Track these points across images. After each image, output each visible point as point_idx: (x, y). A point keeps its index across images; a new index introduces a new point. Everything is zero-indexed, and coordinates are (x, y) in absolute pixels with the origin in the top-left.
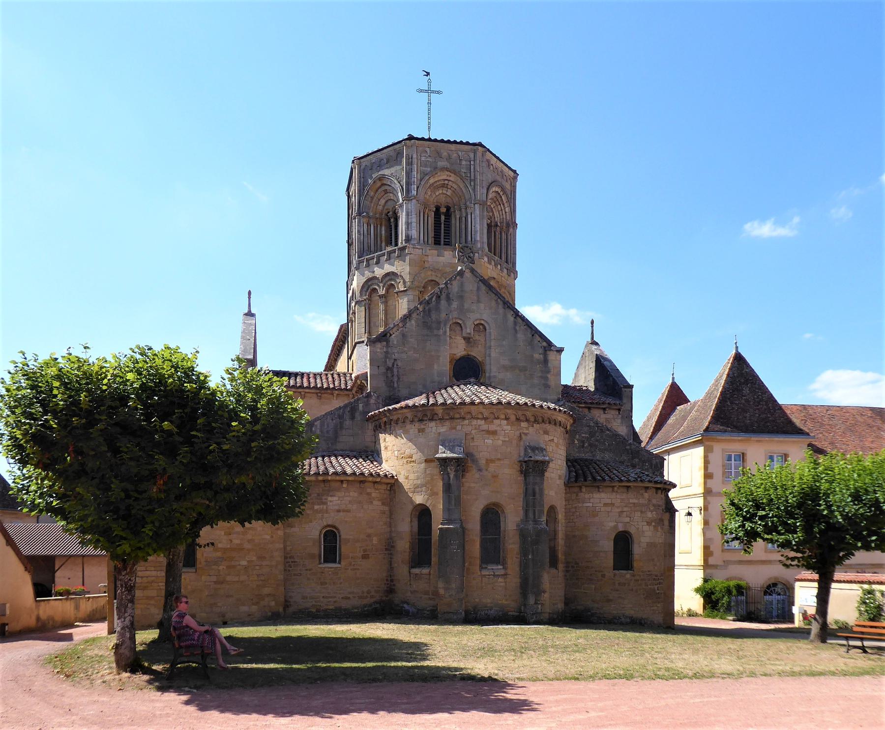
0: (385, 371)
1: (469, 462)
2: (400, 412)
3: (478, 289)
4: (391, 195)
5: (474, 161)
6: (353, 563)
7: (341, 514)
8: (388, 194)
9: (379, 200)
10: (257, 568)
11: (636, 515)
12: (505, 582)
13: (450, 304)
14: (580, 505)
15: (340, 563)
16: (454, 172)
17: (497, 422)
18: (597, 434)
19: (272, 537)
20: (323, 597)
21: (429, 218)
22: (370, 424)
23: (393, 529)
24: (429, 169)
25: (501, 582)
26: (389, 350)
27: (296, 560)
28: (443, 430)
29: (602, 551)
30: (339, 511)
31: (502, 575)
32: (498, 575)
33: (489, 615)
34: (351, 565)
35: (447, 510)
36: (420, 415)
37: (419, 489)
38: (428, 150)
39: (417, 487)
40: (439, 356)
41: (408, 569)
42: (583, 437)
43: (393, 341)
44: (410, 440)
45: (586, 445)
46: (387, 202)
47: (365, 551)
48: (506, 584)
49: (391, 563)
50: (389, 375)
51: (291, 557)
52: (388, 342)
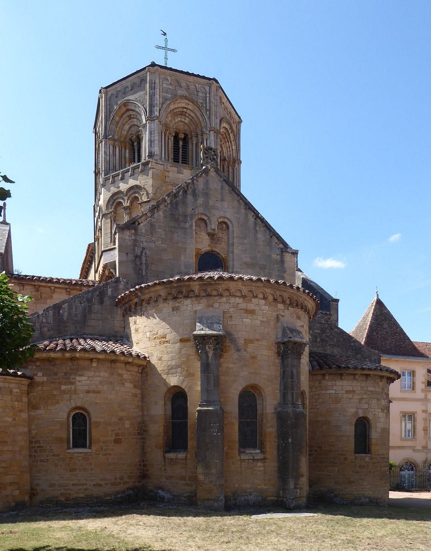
0: (134, 258)
1: (227, 341)
3: (222, 187)
4: (135, 120)
5: (209, 94)
6: (105, 448)
7: (91, 395)
8: (132, 120)
9: (124, 125)
13: (196, 200)
14: (323, 392)
15: (90, 448)
17: (254, 300)
18: (328, 331)
24: (170, 96)
26: (138, 238)
28: (200, 308)
29: (344, 436)
30: (88, 392)
35: (206, 390)
37: (174, 370)
38: (169, 78)
39: (172, 368)
42: (316, 333)
44: (163, 320)
45: (318, 340)
46: (130, 127)
50: (138, 263)
51: (37, 442)
52: (136, 230)
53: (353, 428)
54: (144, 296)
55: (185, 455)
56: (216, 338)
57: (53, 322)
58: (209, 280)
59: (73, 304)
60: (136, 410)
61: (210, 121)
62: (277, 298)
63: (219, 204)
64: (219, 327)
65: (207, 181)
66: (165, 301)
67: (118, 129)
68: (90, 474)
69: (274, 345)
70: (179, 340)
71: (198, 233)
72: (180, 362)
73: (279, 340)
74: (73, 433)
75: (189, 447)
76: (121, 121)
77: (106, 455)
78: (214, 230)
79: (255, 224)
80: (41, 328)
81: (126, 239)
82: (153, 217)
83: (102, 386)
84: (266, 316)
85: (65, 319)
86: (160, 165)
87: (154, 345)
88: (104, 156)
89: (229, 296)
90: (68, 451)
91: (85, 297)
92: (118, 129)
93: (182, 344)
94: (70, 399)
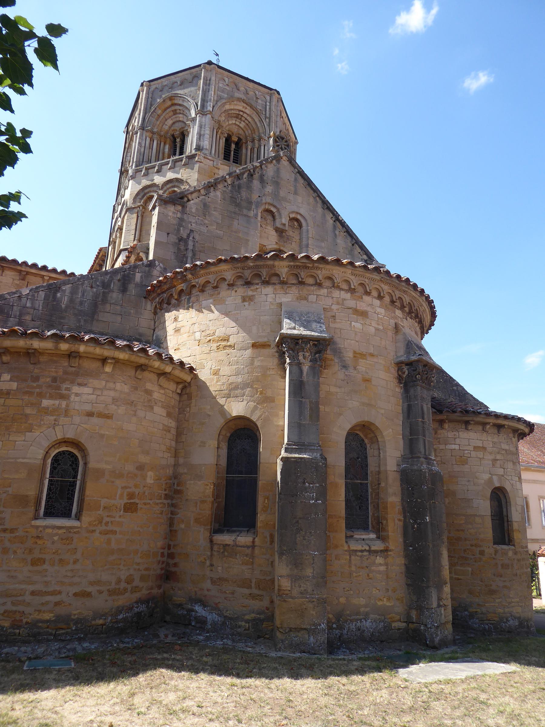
0: (177, 241)
2: (213, 269)
3: (296, 180)
4: (181, 115)
6: (106, 519)
7: (95, 420)
8: (178, 115)
9: (166, 120)
12: (386, 564)
13: (263, 187)
15: (78, 517)
16: (251, 107)
17: (366, 298)
21: (221, 140)
22: (149, 303)
23: (181, 461)
25: (381, 565)
26: (185, 217)
28: (287, 300)
30: (90, 414)
31: (381, 551)
32: (376, 552)
34: (101, 522)
36: (248, 274)
37: (238, 392)
39: (236, 388)
40: (248, 240)
43: (191, 208)
44: (226, 314)
46: (174, 123)
47: (131, 496)
49: (171, 522)
50: (182, 248)
52: (184, 206)
54: (197, 280)
55: (251, 539)
56: (316, 343)
57: (43, 308)
58: (305, 261)
59: (80, 286)
60: (167, 455)
61: (269, 128)
62: (396, 299)
63: (291, 197)
64: (321, 327)
65: (278, 169)
66: (230, 288)
67: (158, 123)
68: (72, 571)
69: (393, 366)
70: (250, 345)
71: (264, 226)
72: (251, 379)
73: (403, 359)
74: (49, 489)
75: (259, 524)
76: (164, 115)
77: (106, 533)
78: (284, 225)
79: (335, 227)
80: (21, 315)
81: (169, 216)
82: (207, 195)
83: (116, 407)
84: (383, 323)
85: (63, 306)
86: (209, 161)
87: (208, 351)
88: (138, 147)
89: (331, 288)
90: (34, 523)
91: (100, 280)
92: (158, 123)
93: (256, 351)
94: (55, 424)
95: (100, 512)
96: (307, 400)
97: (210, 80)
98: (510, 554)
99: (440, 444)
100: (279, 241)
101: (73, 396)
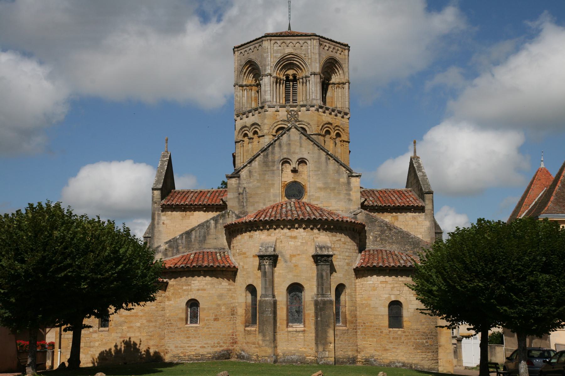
0: (238, 195)
3: (301, 138)
4: (257, 71)
7: (200, 292)
10: (147, 327)
11: (404, 289)
12: (304, 336)
19: (157, 307)
20: (188, 347)
25: (301, 336)
27: (172, 322)
30: (198, 290)
31: (302, 331)
32: (299, 332)
33: (293, 359)
40: (274, 184)
41: (244, 327)
43: (243, 176)
47: (216, 316)
48: (304, 338)
52: (239, 177)
53: (387, 309)
65: (289, 136)
81: (232, 184)
95: (206, 321)
96: (268, 278)
97: (267, 49)
98: (399, 332)
99: (365, 281)
100: (294, 176)
101: (192, 285)
